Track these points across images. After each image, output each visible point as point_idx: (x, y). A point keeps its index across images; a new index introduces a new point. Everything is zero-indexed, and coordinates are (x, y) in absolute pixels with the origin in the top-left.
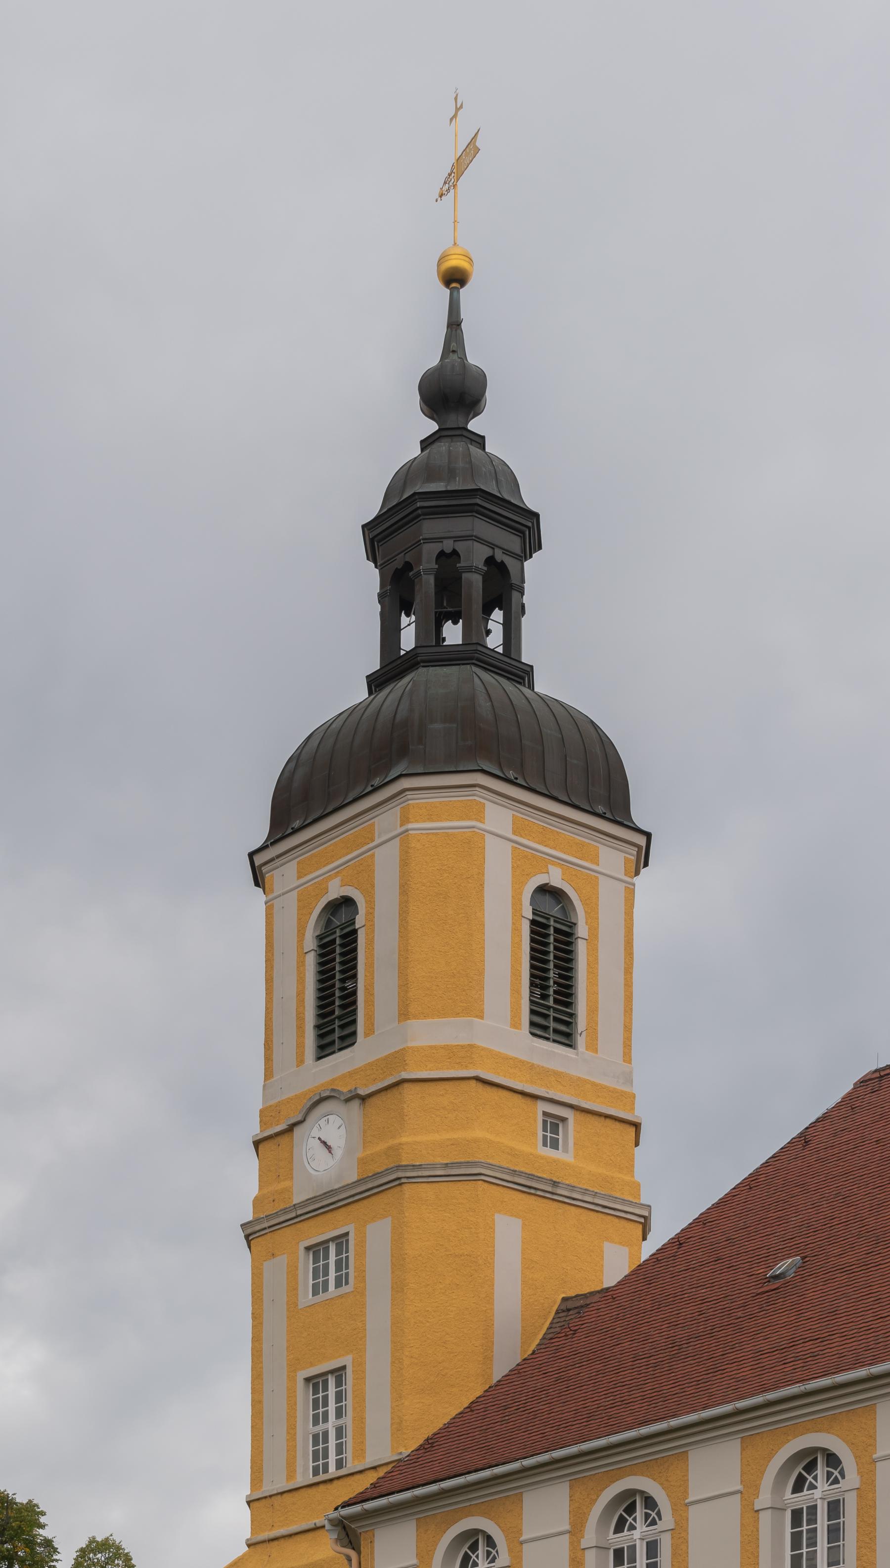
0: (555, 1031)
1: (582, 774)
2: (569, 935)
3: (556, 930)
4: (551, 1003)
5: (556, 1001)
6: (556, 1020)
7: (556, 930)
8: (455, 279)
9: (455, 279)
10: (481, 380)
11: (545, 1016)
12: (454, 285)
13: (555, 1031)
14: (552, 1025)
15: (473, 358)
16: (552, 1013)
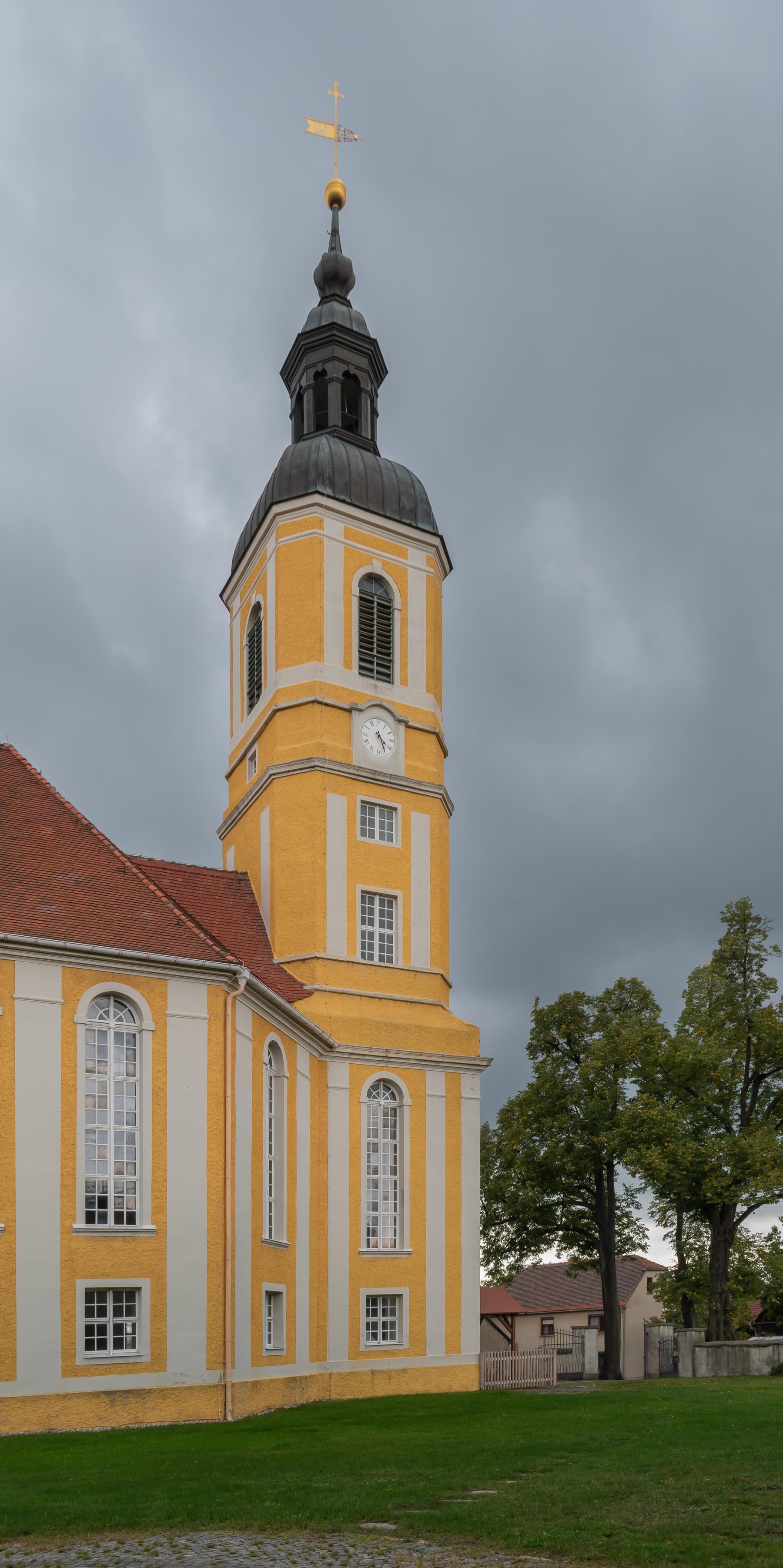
0: (378, 672)
1: (402, 503)
2: (389, 608)
3: (379, 604)
4: (375, 653)
5: (378, 652)
6: (378, 665)
7: (379, 604)
8: (336, 202)
9: (336, 202)
10: (348, 265)
11: (372, 663)
12: (336, 205)
13: (378, 672)
14: (375, 667)
15: (347, 251)
16: (375, 660)
